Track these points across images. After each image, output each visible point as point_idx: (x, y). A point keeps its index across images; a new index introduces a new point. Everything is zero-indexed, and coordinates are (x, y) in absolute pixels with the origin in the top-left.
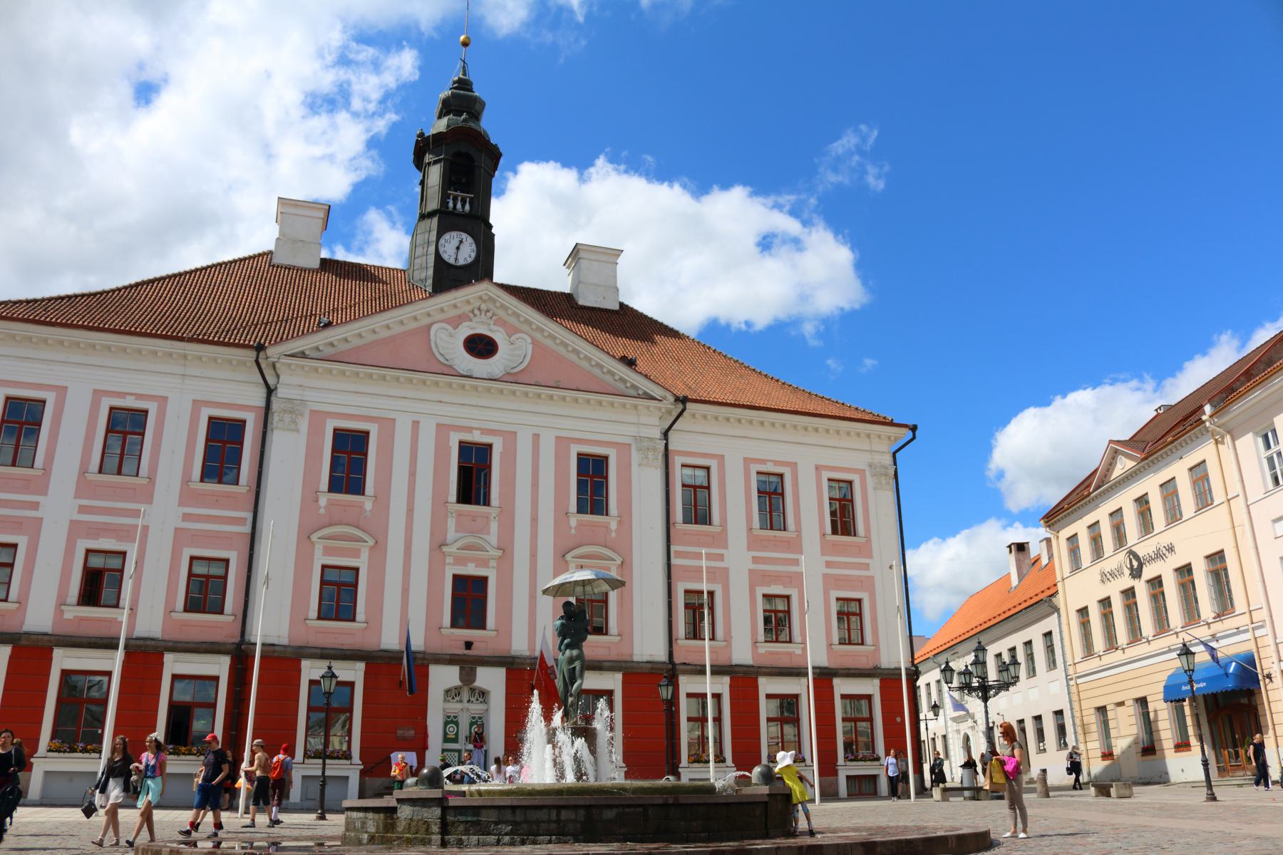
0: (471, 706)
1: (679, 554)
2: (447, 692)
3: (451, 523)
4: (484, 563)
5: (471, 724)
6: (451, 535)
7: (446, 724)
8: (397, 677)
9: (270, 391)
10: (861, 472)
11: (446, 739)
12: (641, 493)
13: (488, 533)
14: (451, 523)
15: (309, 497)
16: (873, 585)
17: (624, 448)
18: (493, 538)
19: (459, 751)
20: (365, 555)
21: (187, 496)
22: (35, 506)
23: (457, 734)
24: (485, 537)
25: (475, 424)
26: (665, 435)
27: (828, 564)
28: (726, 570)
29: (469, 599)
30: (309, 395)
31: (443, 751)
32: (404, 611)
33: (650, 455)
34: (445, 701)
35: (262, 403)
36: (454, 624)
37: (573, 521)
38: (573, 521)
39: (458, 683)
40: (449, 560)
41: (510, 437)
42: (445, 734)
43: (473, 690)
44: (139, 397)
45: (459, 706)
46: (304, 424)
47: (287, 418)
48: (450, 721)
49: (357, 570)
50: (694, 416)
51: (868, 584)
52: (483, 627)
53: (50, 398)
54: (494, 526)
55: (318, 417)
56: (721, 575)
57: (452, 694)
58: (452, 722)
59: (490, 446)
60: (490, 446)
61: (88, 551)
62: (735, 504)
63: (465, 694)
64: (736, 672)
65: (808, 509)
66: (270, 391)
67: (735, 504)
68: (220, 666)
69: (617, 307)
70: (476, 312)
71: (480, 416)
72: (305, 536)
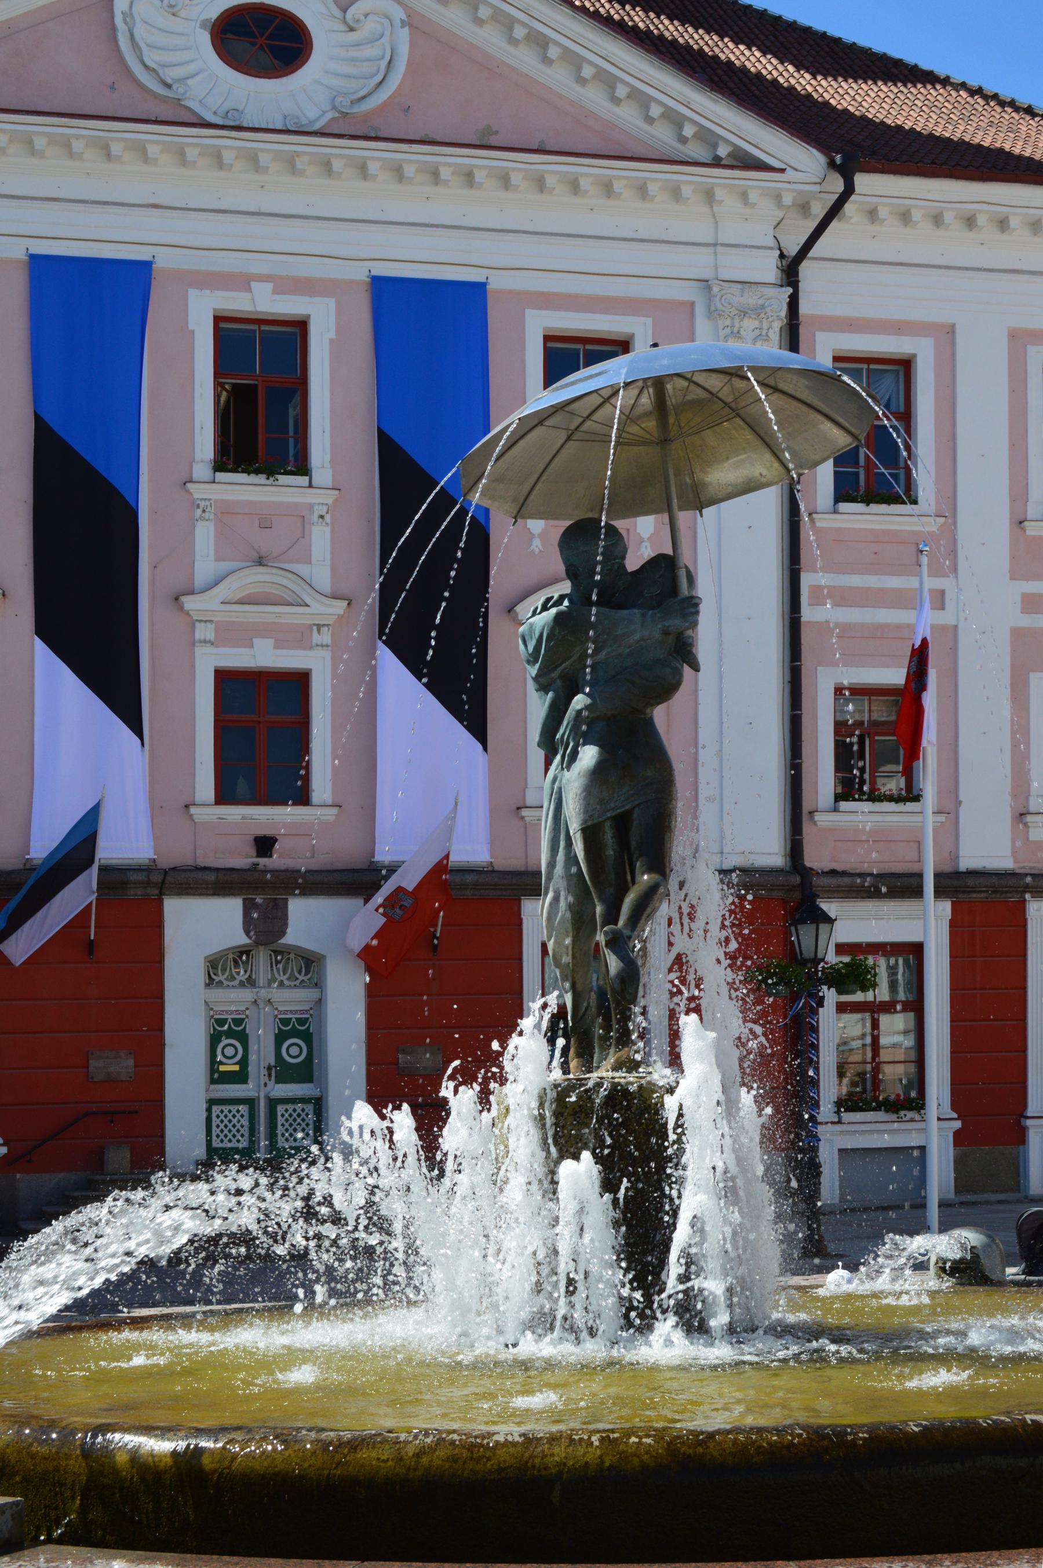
0: (277, 994)
4: (300, 637)
5: (280, 1038)
7: (214, 1040)
11: (217, 1076)
13: (307, 559)
19: (251, 1103)
23: (244, 1063)
24: (301, 569)
25: (258, 265)
26: (791, 271)
34: (210, 982)
36: (224, 796)
39: (241, 939)
40: (203, 632)
42: (213, 1063)
43: (282, 955)
45: (247, 995)
48: (226, 1031)
50: (872, 214)
52: (303, 798)
57: (218, 968)
59: (301, 326)
60: (301, 326)
64: (968, 890)
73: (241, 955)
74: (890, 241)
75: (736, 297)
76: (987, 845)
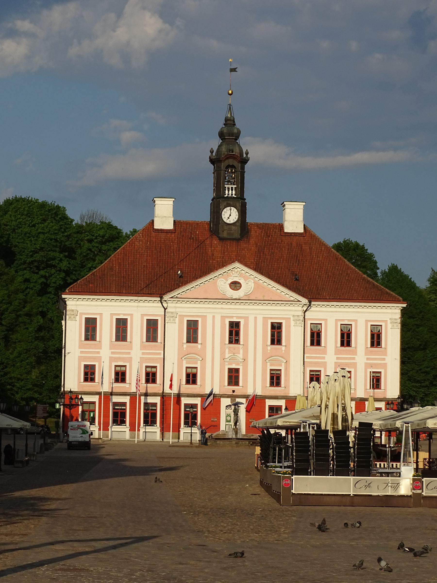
1: (308, 357)
2: (227, 406)
3: (227, 351)
4: (238, 365)
6: (227, 355)
7: (227, 416)
8: (212, 401)
9: (165, 309)
10: (386, 321)
11: (227, 421)
12: (295, 336)
14: (227, 351)
15: (181, 345)
20: (199, 362)
21: (143, 347)
22: (98, 353)
23: (230, 420)
27: (368, 359)
28: (326, 362)
29: (234, 376)
30: (178, 310)
31: (226, 425)
32: (212, 380)
33: (298, 322)
35: (164, 314)
36: (229, 385)
37: (269, 348)
38: (269, 348)
40: (227, 363)
41: (246, 319)
44: (124, 315)
46: (177, 320)
47: (172, 319)
49: (196, 368)
51: (385, 366)
53: (98, 317)
54: (241, 351)
55: (182, 317)
58: (229, 416)
61: (116, 366)
62: (331, 337)
65: (361, 338)
66: (165, 309)
67: (331, 337)
68: (157, 400)
69: (302, 231)
70: (234, 273)
71: (235, 312)
72: (180, 359)
73: (230, 406)
74: (318, 309)
75: (296, 318)
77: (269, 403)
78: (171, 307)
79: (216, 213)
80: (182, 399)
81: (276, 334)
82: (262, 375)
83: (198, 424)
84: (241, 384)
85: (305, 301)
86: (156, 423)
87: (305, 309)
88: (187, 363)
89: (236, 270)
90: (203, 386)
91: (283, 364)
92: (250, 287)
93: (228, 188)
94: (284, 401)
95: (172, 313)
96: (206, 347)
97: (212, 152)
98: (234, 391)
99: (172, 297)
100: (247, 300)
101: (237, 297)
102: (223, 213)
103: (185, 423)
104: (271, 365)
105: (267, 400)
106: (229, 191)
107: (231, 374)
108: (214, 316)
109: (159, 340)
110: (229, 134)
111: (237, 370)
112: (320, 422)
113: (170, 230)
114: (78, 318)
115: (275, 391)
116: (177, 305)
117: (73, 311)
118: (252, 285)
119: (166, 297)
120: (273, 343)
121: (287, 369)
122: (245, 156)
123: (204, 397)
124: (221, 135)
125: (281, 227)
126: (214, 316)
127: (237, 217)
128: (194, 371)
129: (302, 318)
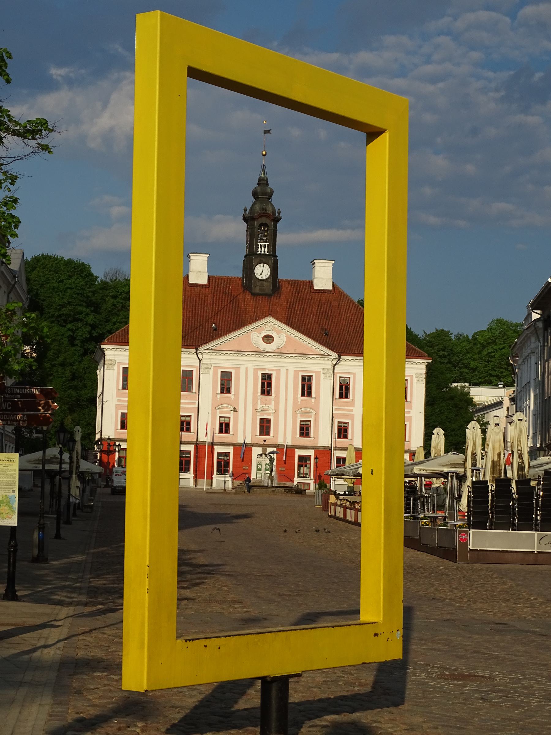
0: (265, 460)
1: (337, 409)
2: (258, 455)
3: (259, 401)
4: (270, 415)
6: (259, 406)
8: (243, 451)
9: (200, 361)
11: (258, 469)
12: (325, 389)
14: (259, 401)
16: (411, 419)
17: (318, 373)
18: (272, 407)
28: (353, 415)
29: (265, 427)
30: (212, 362)
32: (244, 431)
33: (328, 375)
36: (260, 434)
37: (299, 400)
38: (299, 400)
41: (278, 371)
45: (262, 459)
46: (211, 371)
47: (206, 370)
48: (259, 464)
49: (229, 418)
54: (273, 402)
55: (216, 368)
56: (352, 417)
63: (264, 456)
66: (200, 361)
68: (191, 448)
69: (331, 288)
71: (267, 365)
72: (214, 408)
73: (262, 454)
74: (347, 363)
75: (326, 371)
76: (358, 444)
77: (298, 452)
78: (206, 359)
79: (249, 269)
80: (215, 447)
81: (307, 386)
82: (293, 426)
83: (230, 472)
84: (272, 434)
85: (335, 355)
86: (189, 470)
87: (334, 362)
88: (220, 413)
89: (269, 324)
90: (235, 434)
91: (313, 415)
92: (282, 340)
93: (261, 246)
94: (313, 451)
95: (207, 364)
96: (238, 398)
97: (245, 210)
98: (265, 441)
99: (207, 349)
100: (280, 353)
101: (270, 350)
102: (256, 269)
103: (218, 471)
104: (301, 416)
105: (296, 450)
106: (261, 248)
107: (263, 424)
108: (247, 368)
109: (194, 391)
110: (262, 192)
111: (269, 421)
112: (465, 471)
113: (204, 285)
114: (116, 367)
115: (305, 441)
116: (212, 357)
117: (111, 360)
118: (284, 338)
119: (201, 349)
120: (303, 395)
121: (316, 420)
122: (277, 214)
123: (237, 446)
124: (255, 194)
125: (311, 284)
126: (247, 368)
127: (269, 274)
128: (227, 420)
129: (332, 372)
